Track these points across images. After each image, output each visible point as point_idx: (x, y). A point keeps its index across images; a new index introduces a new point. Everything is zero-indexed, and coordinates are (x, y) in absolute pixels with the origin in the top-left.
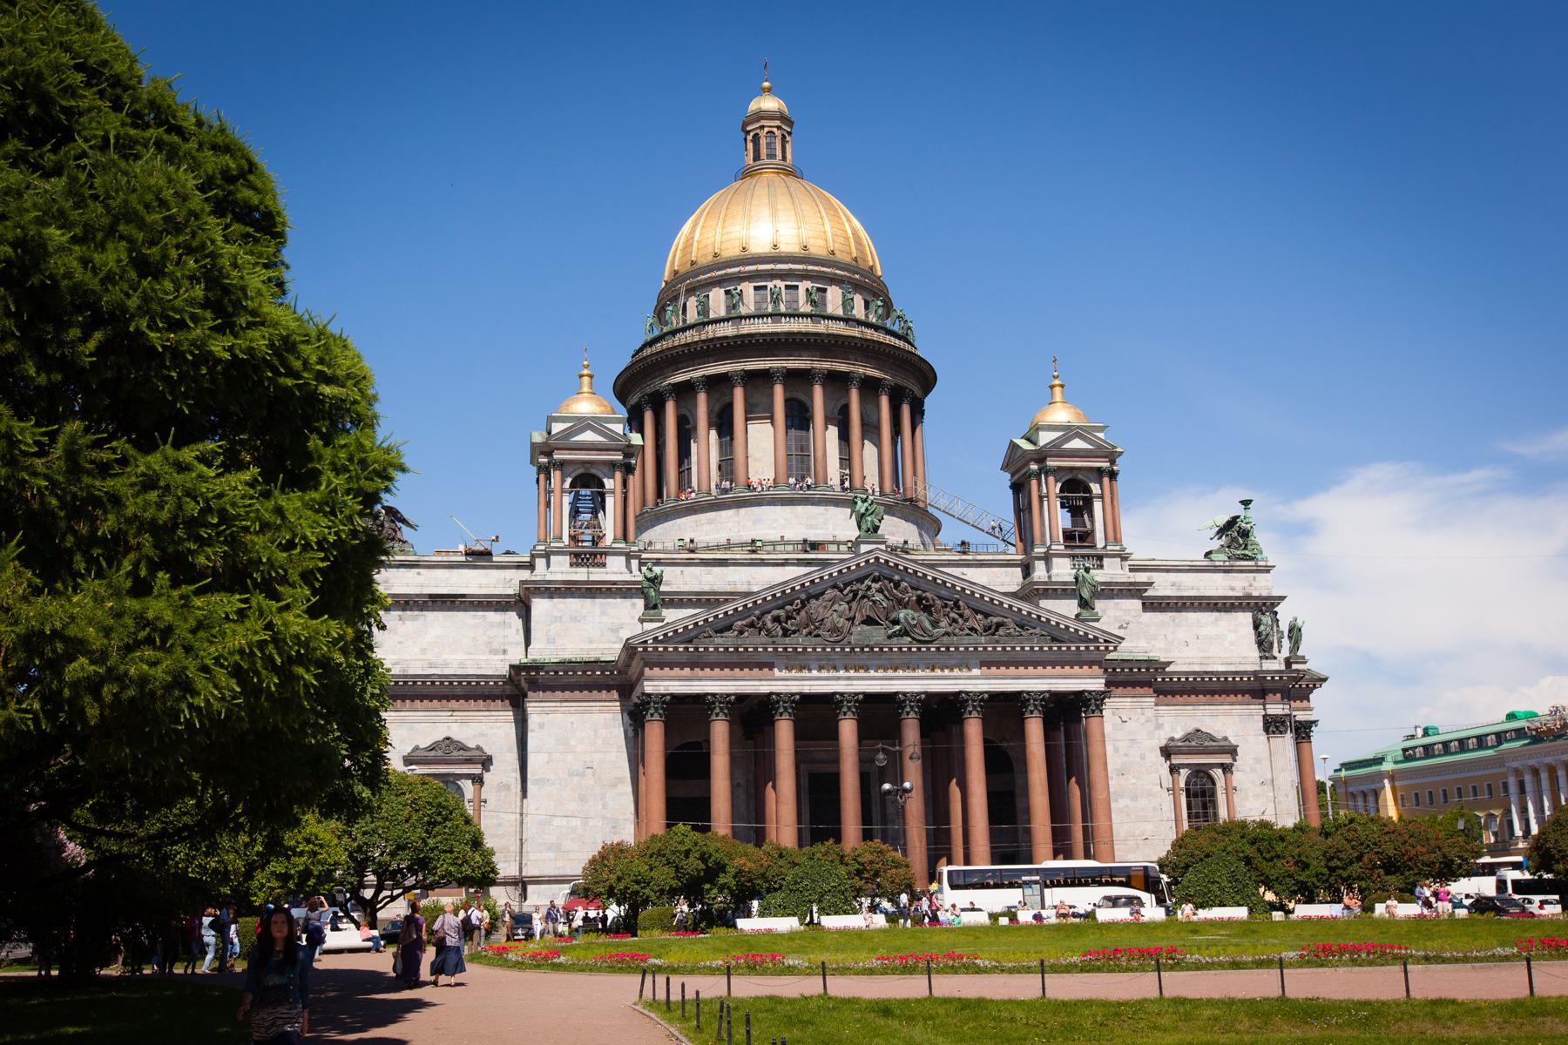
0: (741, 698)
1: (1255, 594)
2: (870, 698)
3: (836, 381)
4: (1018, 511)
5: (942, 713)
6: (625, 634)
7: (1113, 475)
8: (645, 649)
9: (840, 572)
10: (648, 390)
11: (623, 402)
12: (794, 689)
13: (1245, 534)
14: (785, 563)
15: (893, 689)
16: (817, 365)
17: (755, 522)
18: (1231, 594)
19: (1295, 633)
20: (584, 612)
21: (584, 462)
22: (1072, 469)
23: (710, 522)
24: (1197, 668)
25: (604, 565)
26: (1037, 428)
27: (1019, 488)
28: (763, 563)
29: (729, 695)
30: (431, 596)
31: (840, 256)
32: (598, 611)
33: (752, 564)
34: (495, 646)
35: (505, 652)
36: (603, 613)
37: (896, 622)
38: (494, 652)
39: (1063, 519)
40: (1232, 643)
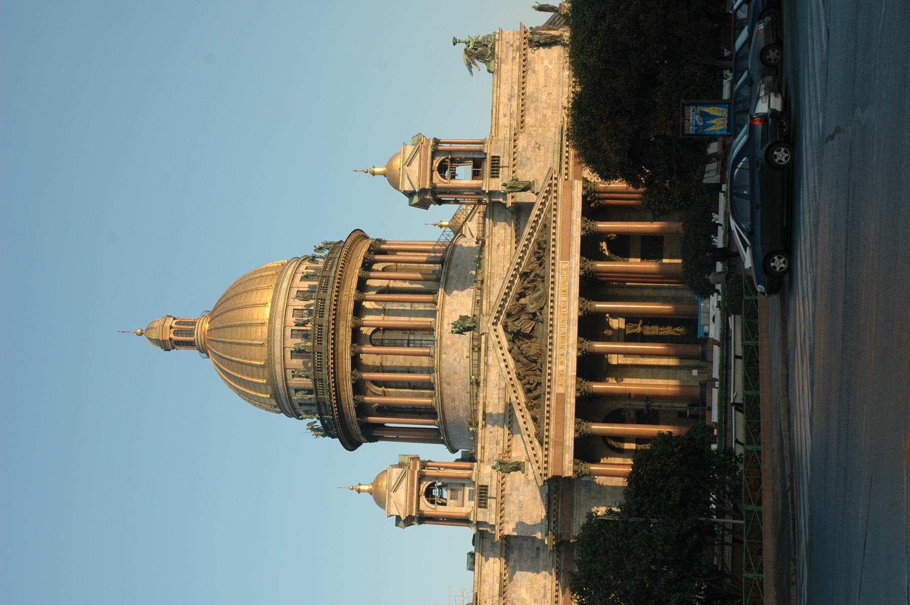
0: (578, 414)
1: (518, 43)
2: (580, 334)
3: (359, 311)
4: (456, 202)
5: (592, 286)
6: (531, 477)
7: (437, 142)
8: (545, 475)
9: (501, 348)
10: (360, 433)
11: (359, 444)
12: (574, 382)
13: (478, 43)
14: (486, 363)
15: (577, 318)
16: (350, 324)
17: (455, 373)
18: (517, 60)
19: (542, 8)
20: (516, 502)
21: (419, 496)
22: (432, 171)
23: (453, 400)
24: (566, 89)
25: (487, 486)
26: (405, 193)
27: (440, 202)
28: (485, 379)
29: (576, 423)
30: (500, 596)
31: (270, 298)
32: (515, 492)
33: (486, 386)
34: (533, 555)
35: (538, 549)
36: (517, 489)
37: (534, 314)
38: (538, 555)
39: (464, 176)
40: (550, 63)
